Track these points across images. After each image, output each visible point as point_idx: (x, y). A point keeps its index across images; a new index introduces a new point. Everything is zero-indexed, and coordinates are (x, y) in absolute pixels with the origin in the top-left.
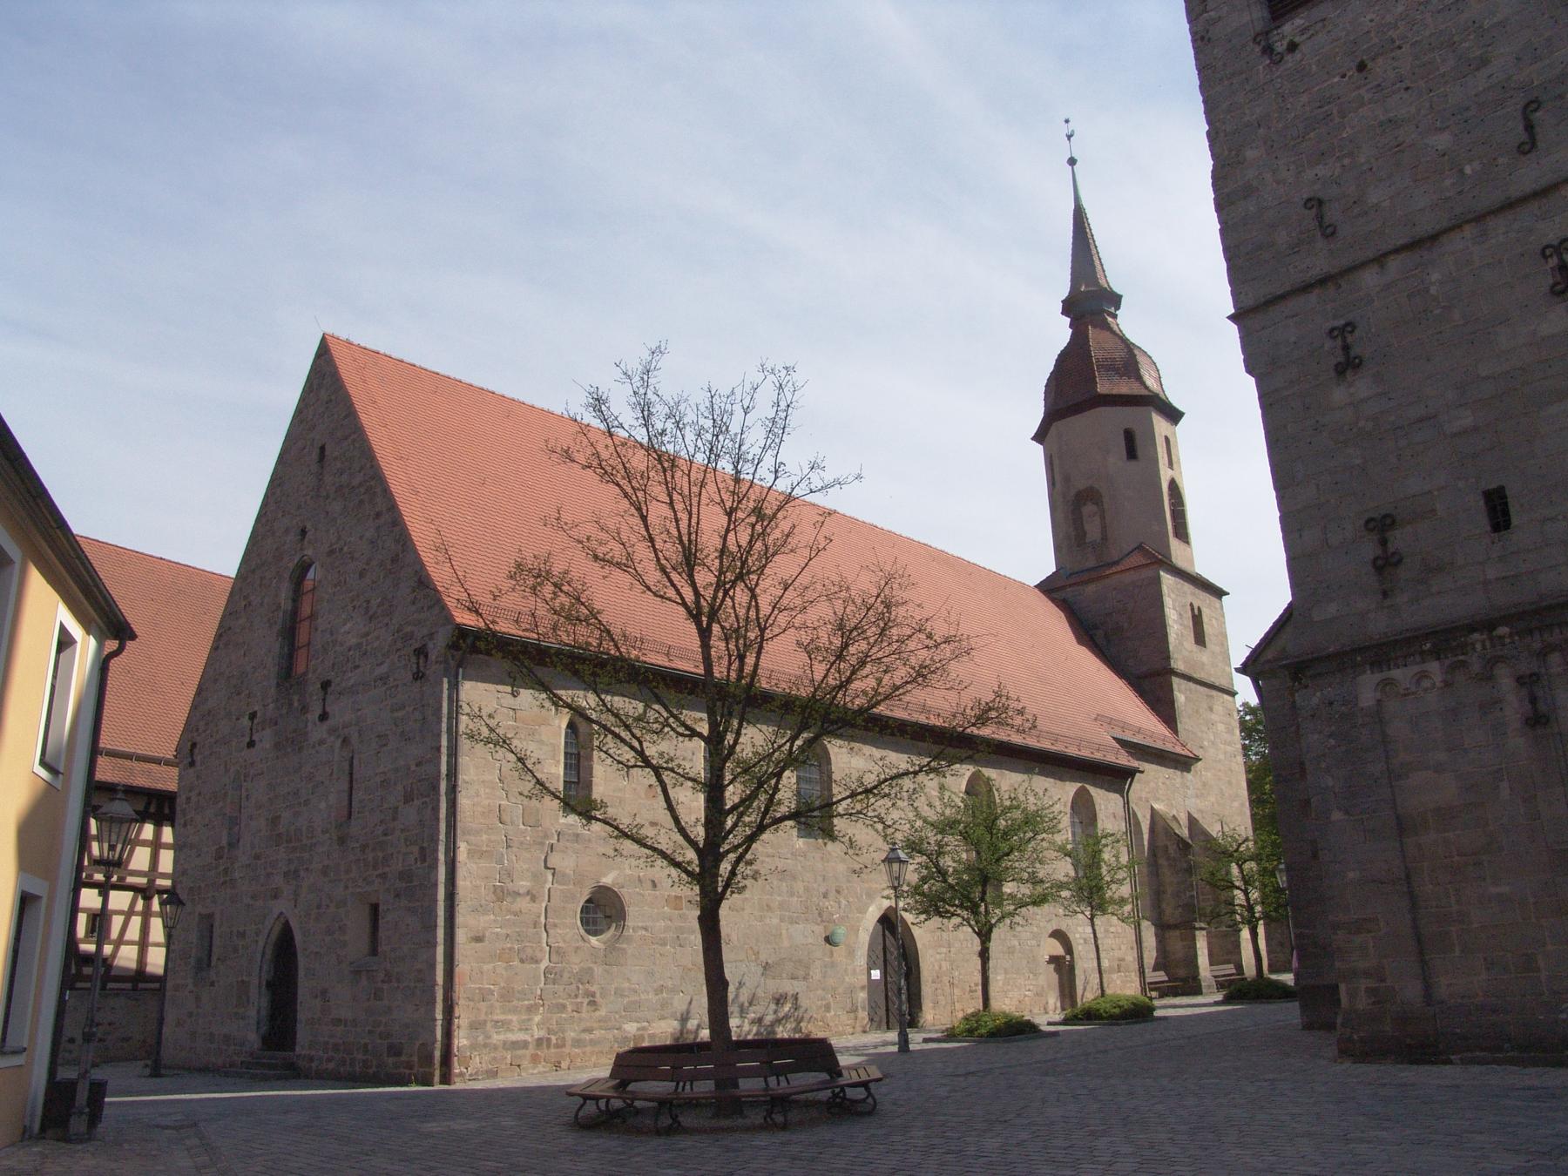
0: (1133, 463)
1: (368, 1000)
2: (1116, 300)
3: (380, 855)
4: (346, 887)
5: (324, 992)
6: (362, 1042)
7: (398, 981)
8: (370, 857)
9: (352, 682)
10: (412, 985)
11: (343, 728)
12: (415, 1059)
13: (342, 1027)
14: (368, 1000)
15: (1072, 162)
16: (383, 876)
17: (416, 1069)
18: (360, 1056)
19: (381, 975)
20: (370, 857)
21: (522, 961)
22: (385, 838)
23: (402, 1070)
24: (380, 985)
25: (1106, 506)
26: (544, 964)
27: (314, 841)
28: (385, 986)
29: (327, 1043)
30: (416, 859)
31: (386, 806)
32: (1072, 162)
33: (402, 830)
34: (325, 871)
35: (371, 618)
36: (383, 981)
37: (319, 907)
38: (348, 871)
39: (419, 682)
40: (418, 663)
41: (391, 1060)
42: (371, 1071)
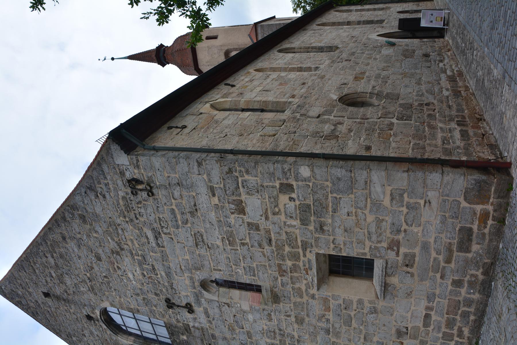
0: (219, 38)
1: (412, 275)
2: (161, 46)
3: (287, 249)
4: (313, 297)
5: (400, 334)
6: (450, 287)
7: (399, 231)
8: (289, 263)
9: (163, 274)
10: (405, 210)
11: (195, 288)
12: (479, 208)
13: (432, 313)
14: (412, 275)
15: (113, 59)
16: (305, 246)
17: (490, 208)
18: (463, 291)
19: (391, 255)
20: (289, 263)
21: (391, 129)
22: (274, 243)
23: (486, 231)
24: (400, 258)
25: (232, 47)
26: (394, 121)
27: (277, 331)
28: (402, 250)
29: (444, 333)
30: (291, 199)
31: (248, 240)
32: (113, 59)
33: (267, 218)
34: (300, 321)
35: (122, 249)
36: (398, 254)
37: (328, 332)
38: (299, 293)
39: (154, 191)
40: (141, 190)
41: (475, 247)
42: (481, 277)
